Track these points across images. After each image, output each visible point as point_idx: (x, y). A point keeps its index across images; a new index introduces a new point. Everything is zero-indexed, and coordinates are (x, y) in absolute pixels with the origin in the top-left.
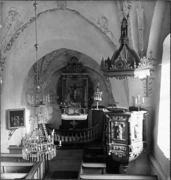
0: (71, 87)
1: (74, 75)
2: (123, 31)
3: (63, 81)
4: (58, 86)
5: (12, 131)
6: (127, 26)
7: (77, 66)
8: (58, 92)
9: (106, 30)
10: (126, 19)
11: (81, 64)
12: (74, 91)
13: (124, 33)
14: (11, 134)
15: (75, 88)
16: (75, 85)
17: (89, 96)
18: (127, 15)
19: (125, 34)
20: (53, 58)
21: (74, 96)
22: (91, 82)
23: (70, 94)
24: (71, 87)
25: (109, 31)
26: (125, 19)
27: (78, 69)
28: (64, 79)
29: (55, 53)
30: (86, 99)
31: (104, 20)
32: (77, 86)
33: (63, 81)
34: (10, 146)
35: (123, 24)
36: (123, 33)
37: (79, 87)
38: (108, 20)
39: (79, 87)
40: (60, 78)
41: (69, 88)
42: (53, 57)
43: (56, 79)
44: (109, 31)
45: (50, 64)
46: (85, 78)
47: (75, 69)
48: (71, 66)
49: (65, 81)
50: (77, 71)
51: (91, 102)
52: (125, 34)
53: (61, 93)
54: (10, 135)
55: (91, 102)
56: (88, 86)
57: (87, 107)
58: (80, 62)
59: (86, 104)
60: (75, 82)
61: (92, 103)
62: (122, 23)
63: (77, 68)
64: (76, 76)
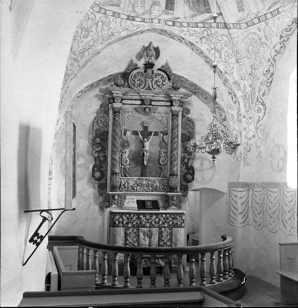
0: (135, 133)
1: (143, 97)
3: (111, 112)
4: (96, 127)
5: (45, 219)
7: (155, 72)
8: (93, 143)
11: (165, 70)
12: (142, 143)
14: (36, 234)
15: (146, 133)
16: (146, 128)
17: (183, 158)
20: (91, 44)
21: (144, 155)
22: (191, 121)
23: (130, 151)
24: (135, 133)
27: (158, 81)
28: (117, 105)
29: (99, 29)
30: (178, 168)
32: (151, 129)
33: (111, 112)
34: (27, 295)
37: (156, 134)
39: (156, 134)
40: (102, 106)
41: (128, 133)
42: (89, 38)
43: (91, 106)
45: (79, 58)
46: (175, 108)
47: (149, 81)
48: (138, 73)
49: (116, 112)
50: (155, 87)
51: (189, 177)
53: (104, 149)
54: (31, 240)
55: (189, 177)
56: (182, 134)
57: (178, 189)
58: (167, 64)
59: (176, 181)
60: (145, 118)
61: (193, 178)
63: (156, 77)
64: (151, 101)
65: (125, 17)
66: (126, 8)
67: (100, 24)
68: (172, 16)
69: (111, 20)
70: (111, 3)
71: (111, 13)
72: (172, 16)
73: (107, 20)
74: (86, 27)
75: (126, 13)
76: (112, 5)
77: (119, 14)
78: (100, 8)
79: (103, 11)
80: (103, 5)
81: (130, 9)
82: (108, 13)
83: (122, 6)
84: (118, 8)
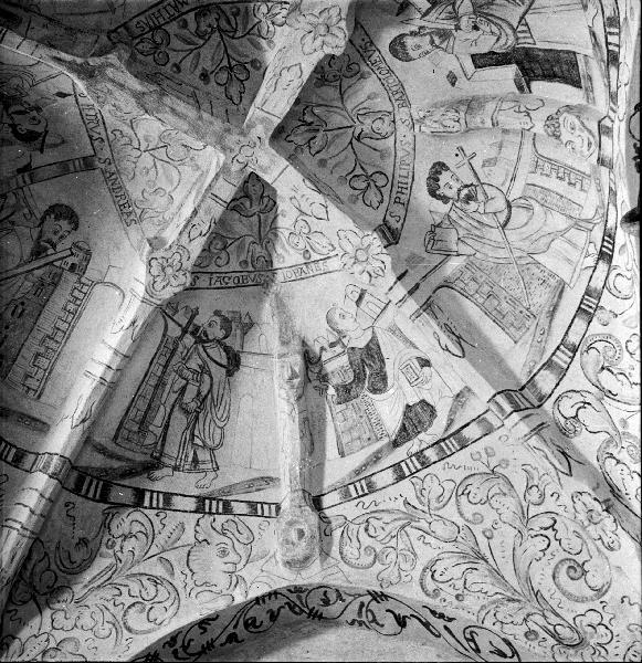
65: (602, 266)
66: (575, 255)
67: (605, 378)
68: (594, 64)
69: (605, 330)
70: (543, 320)
71: (580, 324)
72: (594, 64)
73: (599, 346)
74: (603, 436)
75: (590, 261)
76: (552, 314)
77: (588, 292)
78: (549, 365)
79: (562, 359)
80: (543, 351)
81: (580, 237)
82: (573, 338)
83: (564, 273)
84: (567, 289)
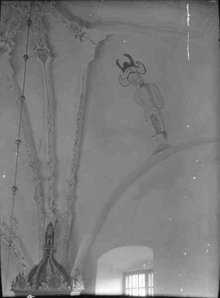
2: (48, 239)
6: (53, 233)
9: (13, 235)
10: (54, 225)
13: (50, 240)
18: (56, 220)
19: (52, 243)
25: (17, 237)
26: (52, 225)
31: (13, 220)
35: (49, 230)
36: (48, 242)
38: (18, 222)
44: (17, 237)
52: (52, 243)
62: (48, 229)
